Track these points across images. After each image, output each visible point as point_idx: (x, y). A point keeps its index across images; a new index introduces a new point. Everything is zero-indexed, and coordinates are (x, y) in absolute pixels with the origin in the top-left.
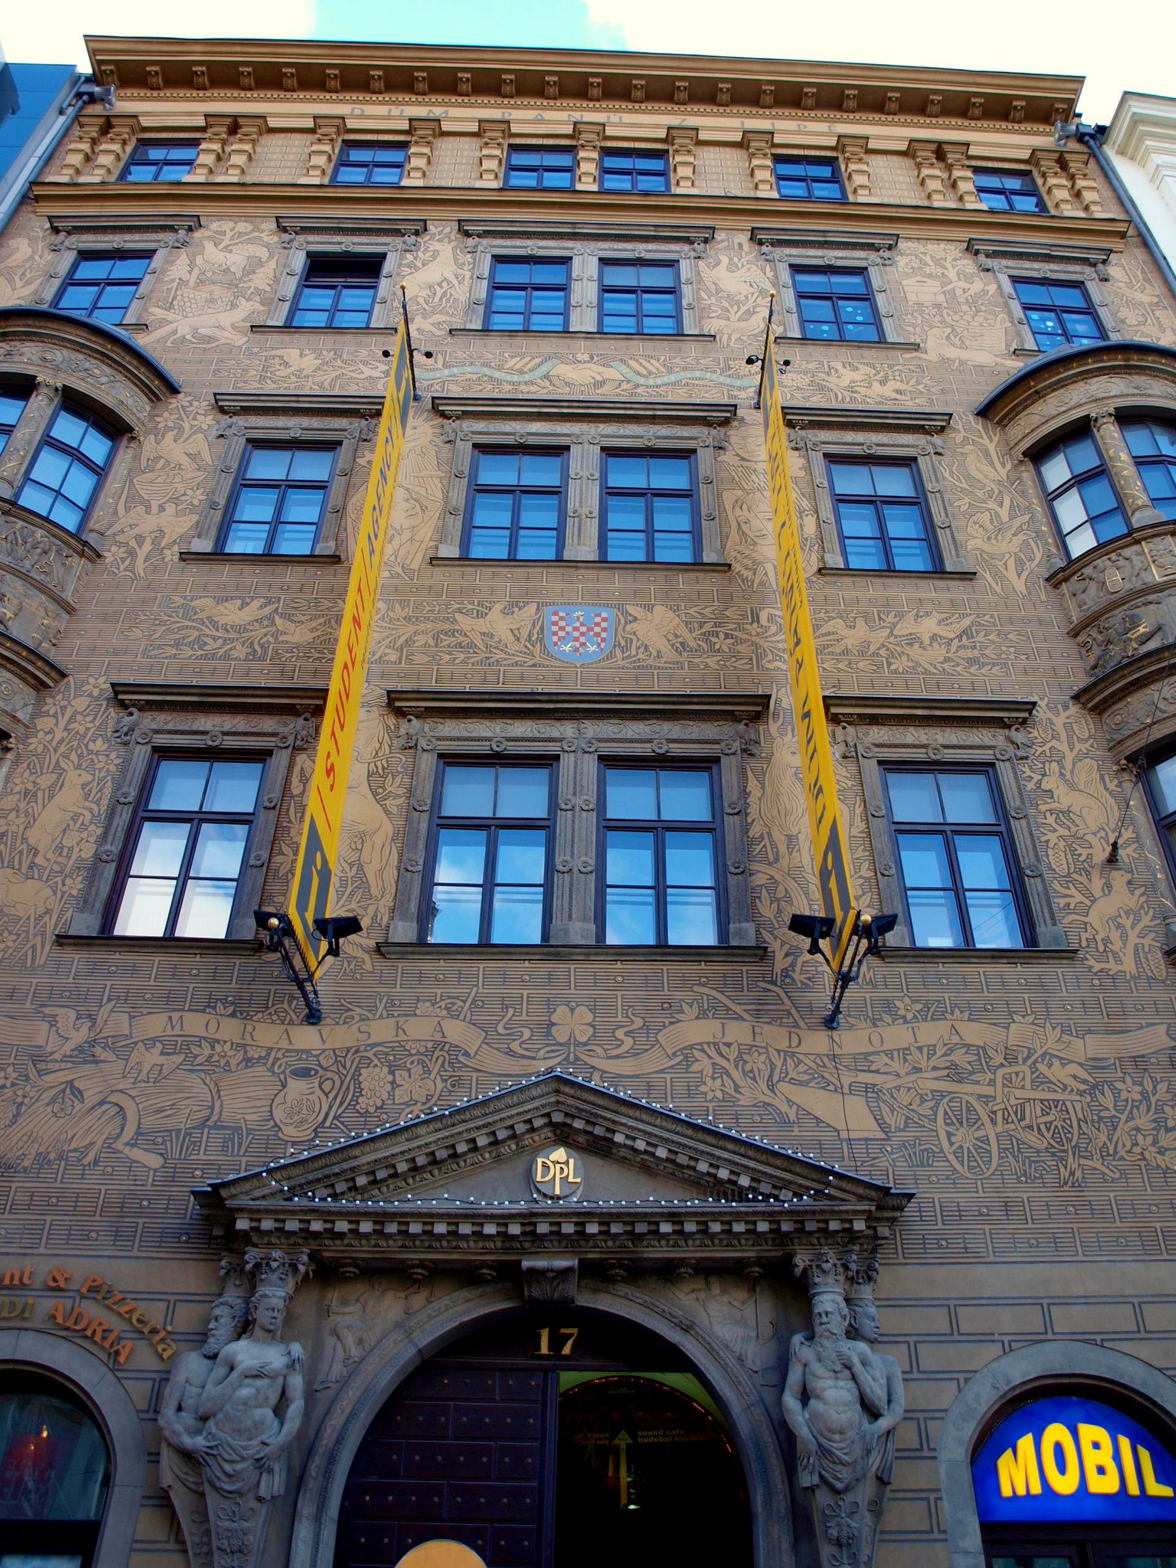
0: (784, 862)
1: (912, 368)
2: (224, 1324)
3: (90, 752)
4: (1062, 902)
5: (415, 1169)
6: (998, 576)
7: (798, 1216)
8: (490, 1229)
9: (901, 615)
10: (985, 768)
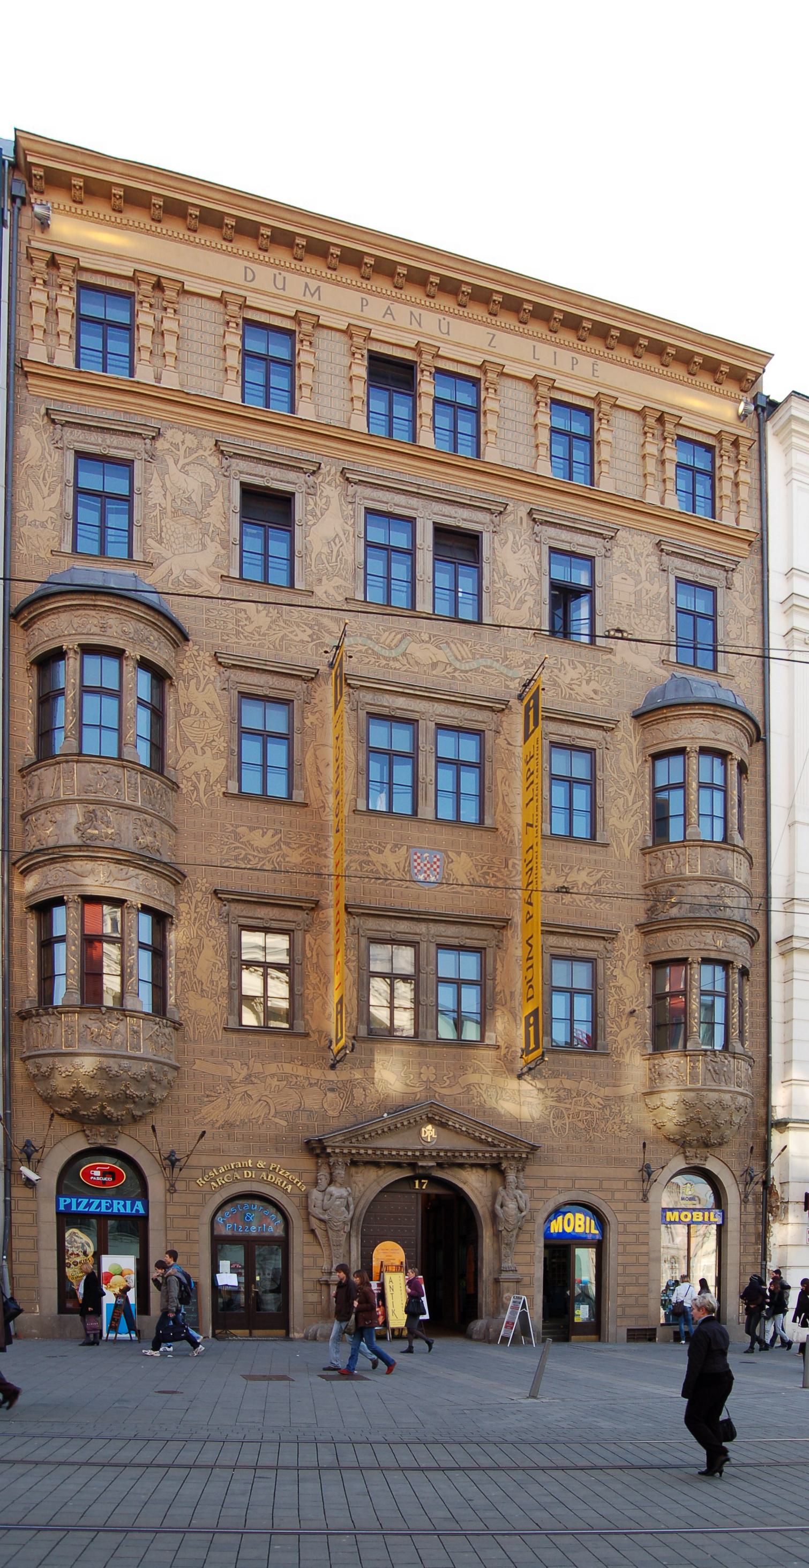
0: (508, 1004)
1: (606, 669)
2: (323, 1181)
3: (211, 927)
4: (609, 1030)
5: (383, 1132)
6: (619, 846)
7: (506, 1152)
8: (410, 1153)
9: (571, 868)
10: (592, 961)
